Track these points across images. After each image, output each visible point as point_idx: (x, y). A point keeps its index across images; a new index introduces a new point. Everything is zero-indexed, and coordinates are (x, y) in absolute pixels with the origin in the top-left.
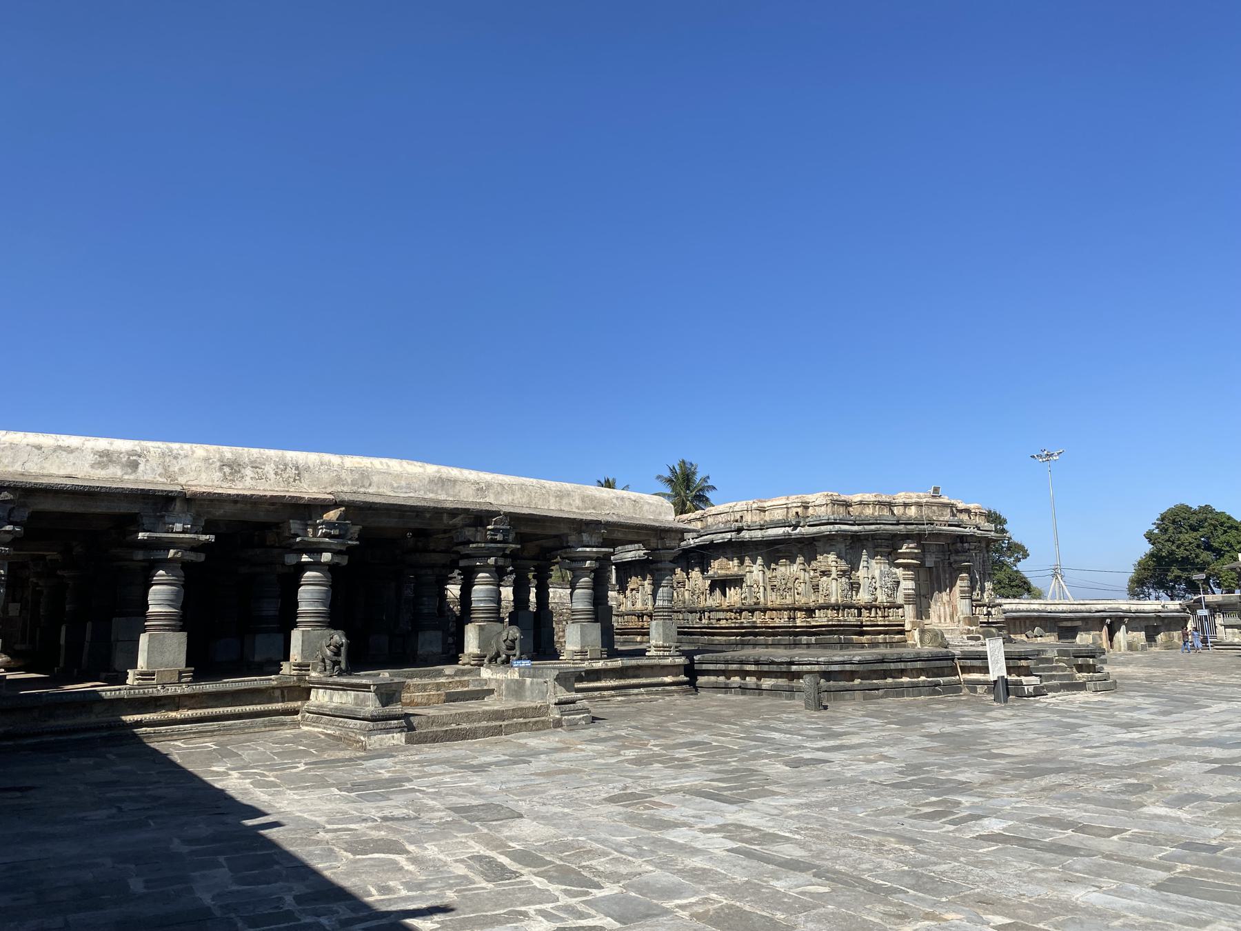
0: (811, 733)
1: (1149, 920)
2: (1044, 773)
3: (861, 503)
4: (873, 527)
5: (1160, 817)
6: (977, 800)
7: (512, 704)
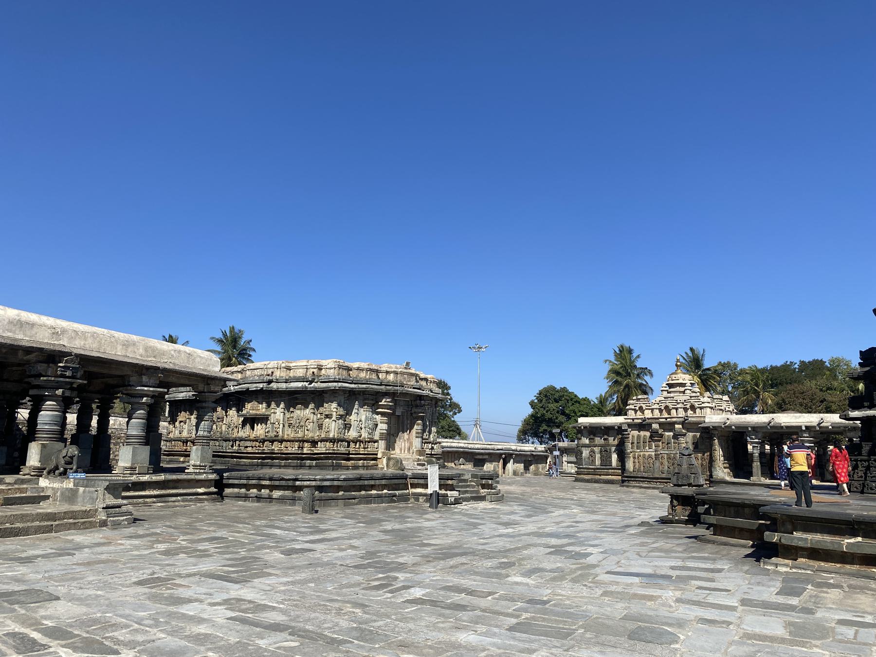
0: (303, 530)
1: (502, 651)
3: (358, 369)
4: (364, 386)
5: (517, 583)
6: (408, 575)
7: (65, 507)
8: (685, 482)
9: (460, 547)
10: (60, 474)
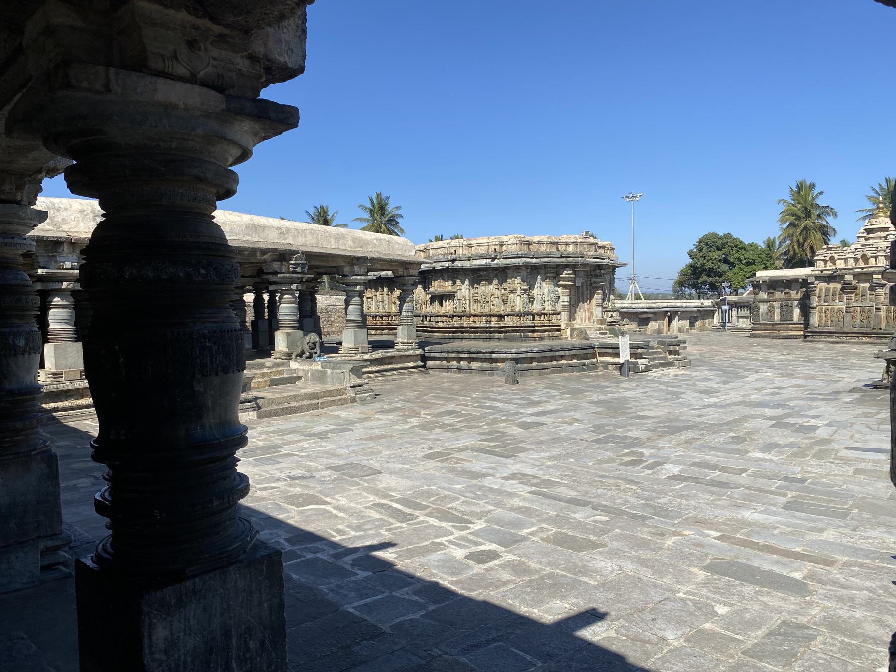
1: (791, 529)
2: (679, 430)
3: (538, 243)
4: (546, 260)
6: (652, 451)
7: (316, 388)
9: (677, 420)
10: (307, 358)
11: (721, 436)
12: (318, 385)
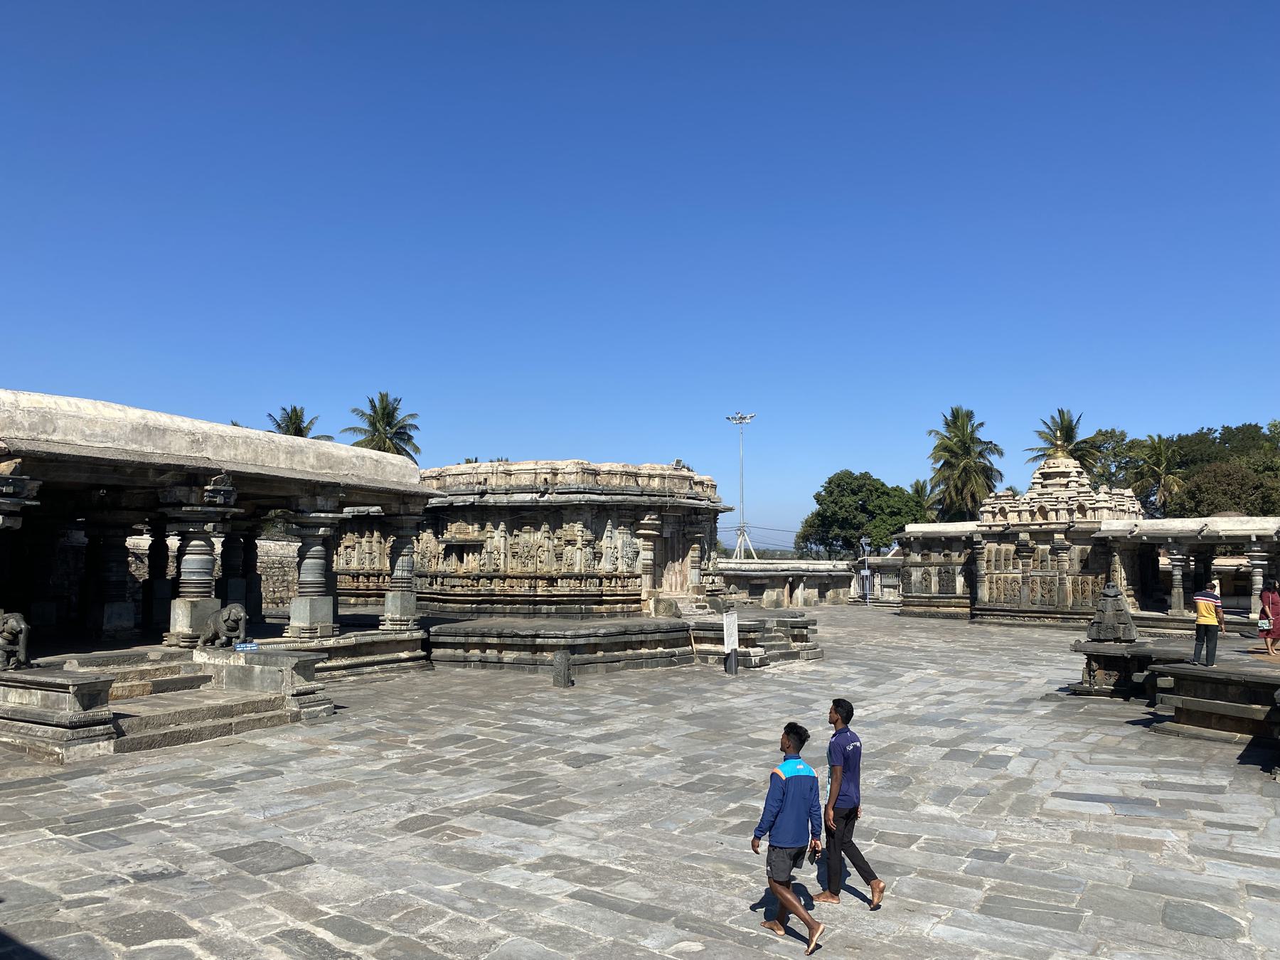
3: (609, 473)
4: (619, 498)
8: (1110, 636)
10: (222, 645)
11: (874, 776)
12: (237, 691)
